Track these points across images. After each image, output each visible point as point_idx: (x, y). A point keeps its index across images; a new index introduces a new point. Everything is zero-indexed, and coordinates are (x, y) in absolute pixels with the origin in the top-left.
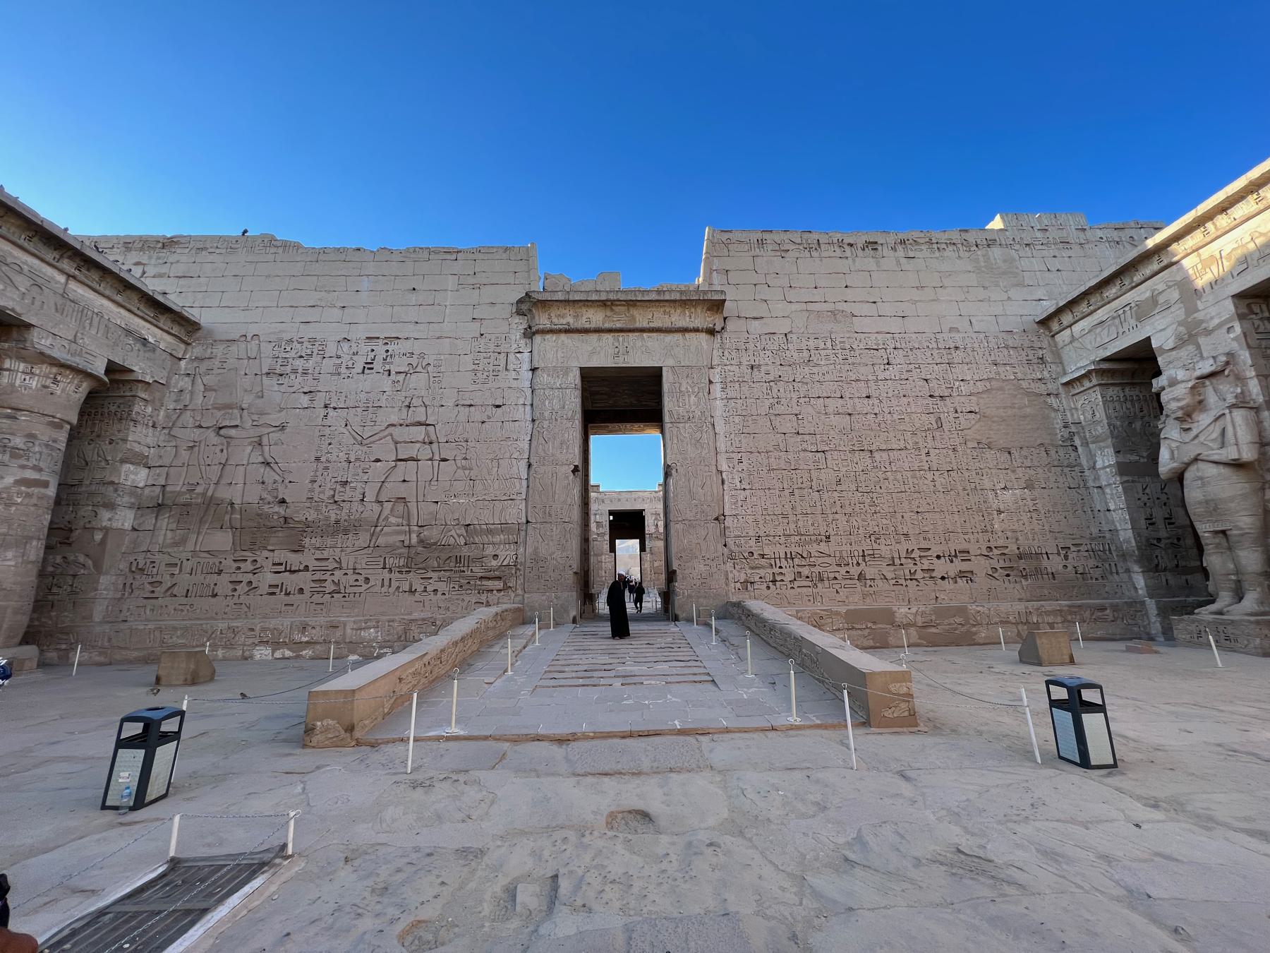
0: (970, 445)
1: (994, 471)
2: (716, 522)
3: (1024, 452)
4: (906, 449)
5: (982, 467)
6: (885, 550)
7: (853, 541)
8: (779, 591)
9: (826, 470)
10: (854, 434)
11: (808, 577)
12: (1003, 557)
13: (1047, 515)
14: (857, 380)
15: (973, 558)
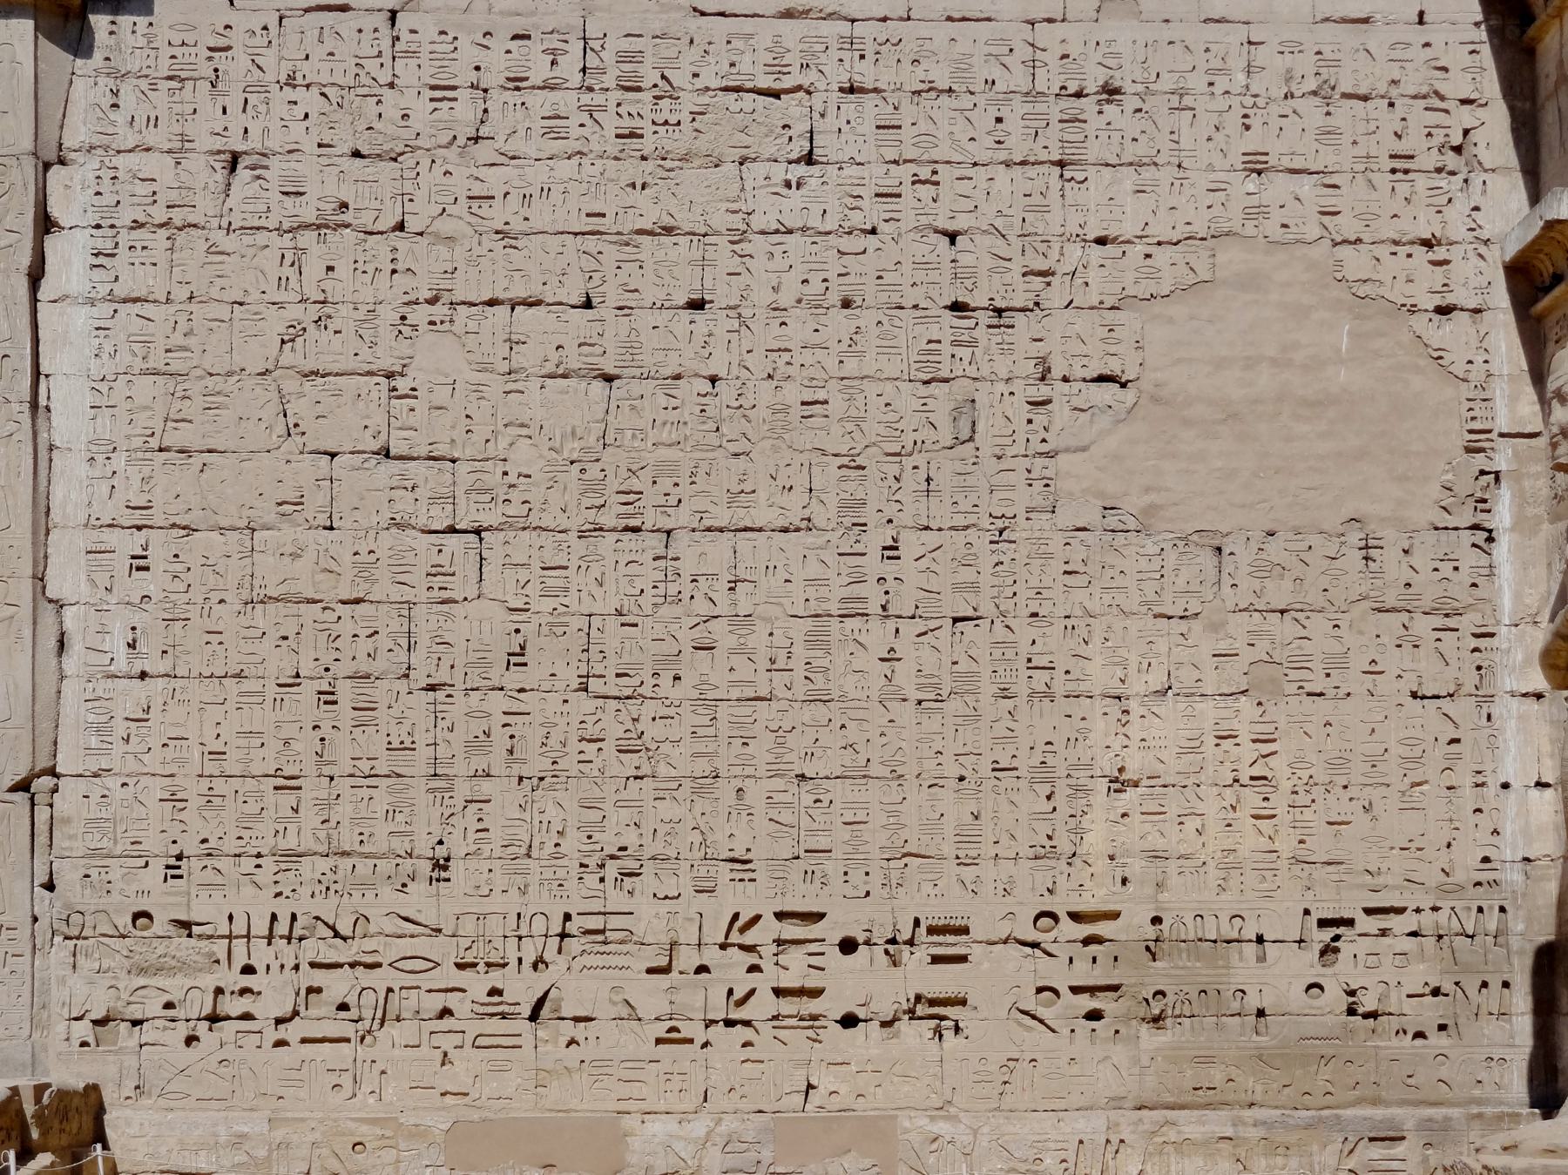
0: (1066, 518)
1: (1134, 625)
2: (20, 797)
3: (1274, 549)
4: (809, 525)
5: (1094, 606)
6: (650, 920)
7: (534, 880)
8: (229, 1052)
9: (483, 602)
10: (607, 456)
11: (343, 1007)
12: (1093, 948)
13: (1302, 799)
14: (669, 230)
15: (976, 952)
